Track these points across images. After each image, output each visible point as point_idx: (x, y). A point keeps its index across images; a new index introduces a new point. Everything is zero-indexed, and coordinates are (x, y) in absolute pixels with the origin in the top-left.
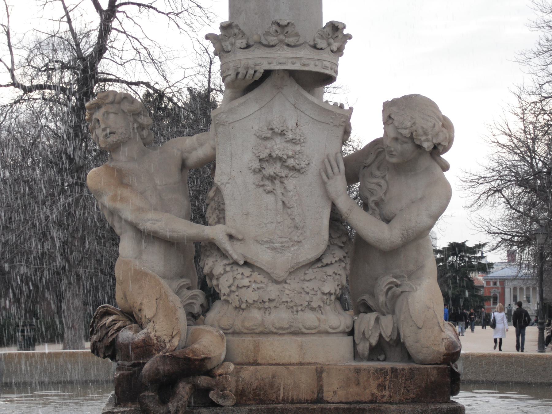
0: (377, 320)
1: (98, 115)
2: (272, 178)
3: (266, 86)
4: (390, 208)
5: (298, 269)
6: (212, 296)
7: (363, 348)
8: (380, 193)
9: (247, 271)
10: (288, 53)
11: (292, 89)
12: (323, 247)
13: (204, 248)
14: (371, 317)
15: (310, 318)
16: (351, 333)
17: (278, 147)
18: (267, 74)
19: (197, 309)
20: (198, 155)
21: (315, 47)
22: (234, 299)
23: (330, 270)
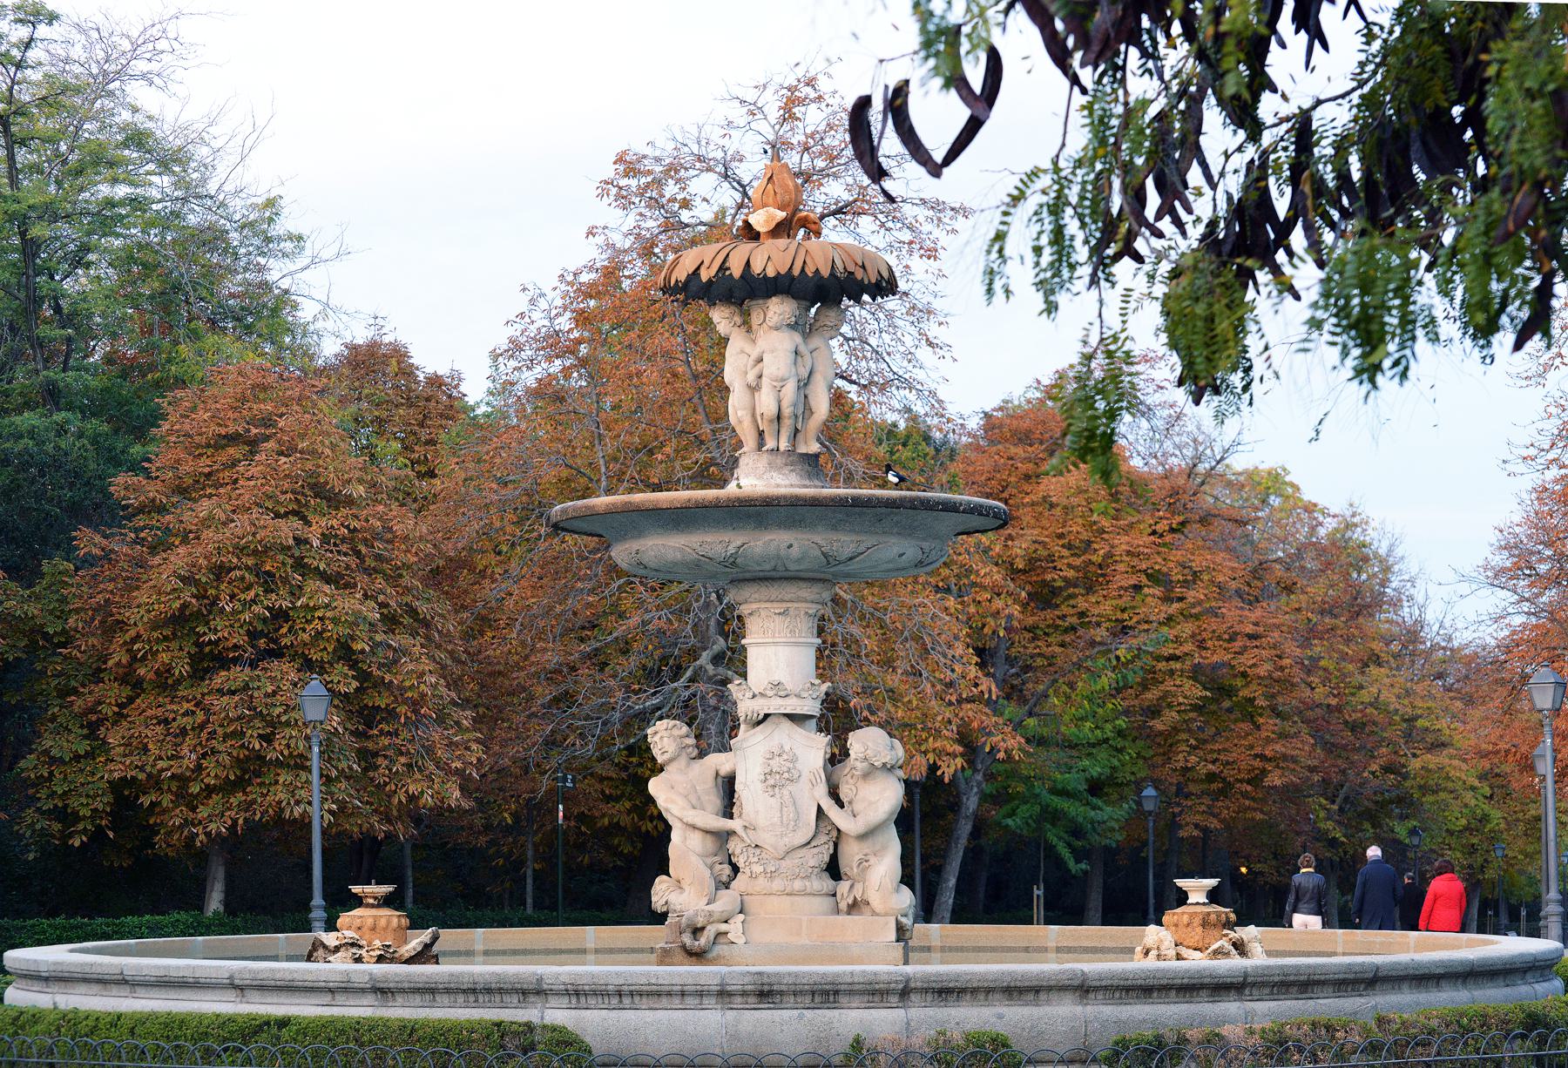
0: (852, 886)
1: (656, 738)
4: (857, 807)
6: (736, 869)
7: (843, 906)
8: (851, 795)
9: (758, 851)
10: (780, 701)
12: (811, 834)
13: (730, 833)
14: (848, 883)
15: (798, 885)
16: (834, 895)
17: (775, 764)
18: (767, 716)
19: (724, 878)
20: (725, 770)
22: (747, 870)
23: (815, 851)
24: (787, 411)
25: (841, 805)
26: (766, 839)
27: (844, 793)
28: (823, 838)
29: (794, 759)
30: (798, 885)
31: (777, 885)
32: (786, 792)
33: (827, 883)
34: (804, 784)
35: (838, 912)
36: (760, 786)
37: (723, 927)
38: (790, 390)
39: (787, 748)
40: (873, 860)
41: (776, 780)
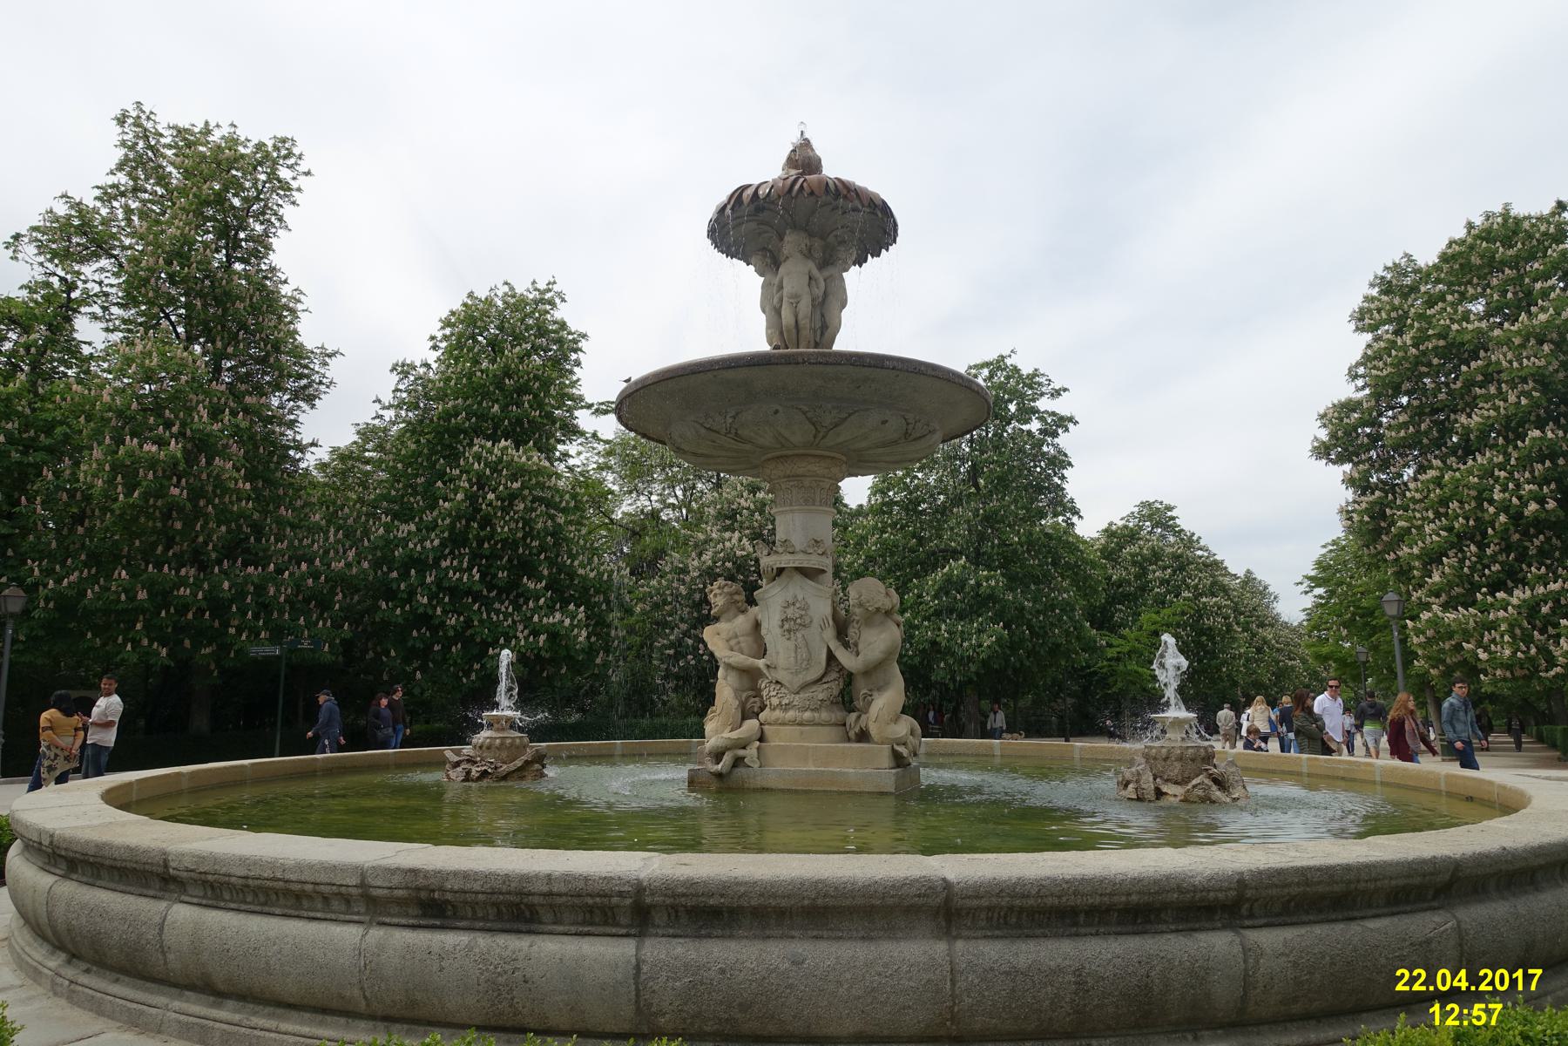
2: (789, 631)
3: (784, 575)
5: (805, 687)
7: (852, 734)
10: (789, 557)
11: (798, 578)
15: (807, 715)
17: (790, 612)
21: (805, 552)
24: (804, 322)
25: (846, 645)
26: (781, 675)
27: (851, 639)
28: (834, 675)
29: (806, 608)
30: (807, 715)
31: (791, 714)
32: (799, 635)
33: (838, 715)
34: (815, 629)
35: (849, 740)
36: (779, 631)
37: (741, 753)
38: (805, 306)
39: (800, 598)
40: (875, 694)
41: (793, 625)
